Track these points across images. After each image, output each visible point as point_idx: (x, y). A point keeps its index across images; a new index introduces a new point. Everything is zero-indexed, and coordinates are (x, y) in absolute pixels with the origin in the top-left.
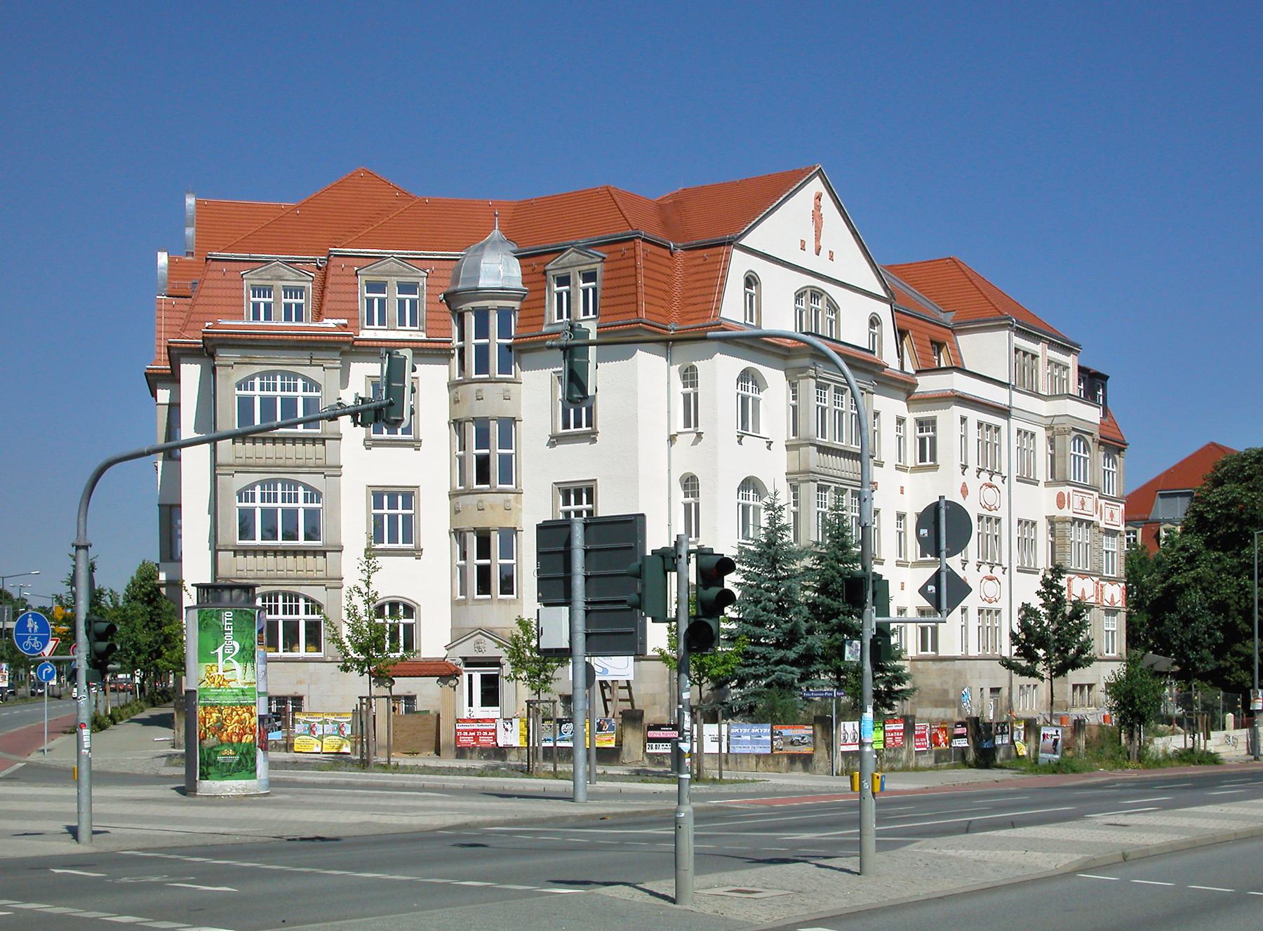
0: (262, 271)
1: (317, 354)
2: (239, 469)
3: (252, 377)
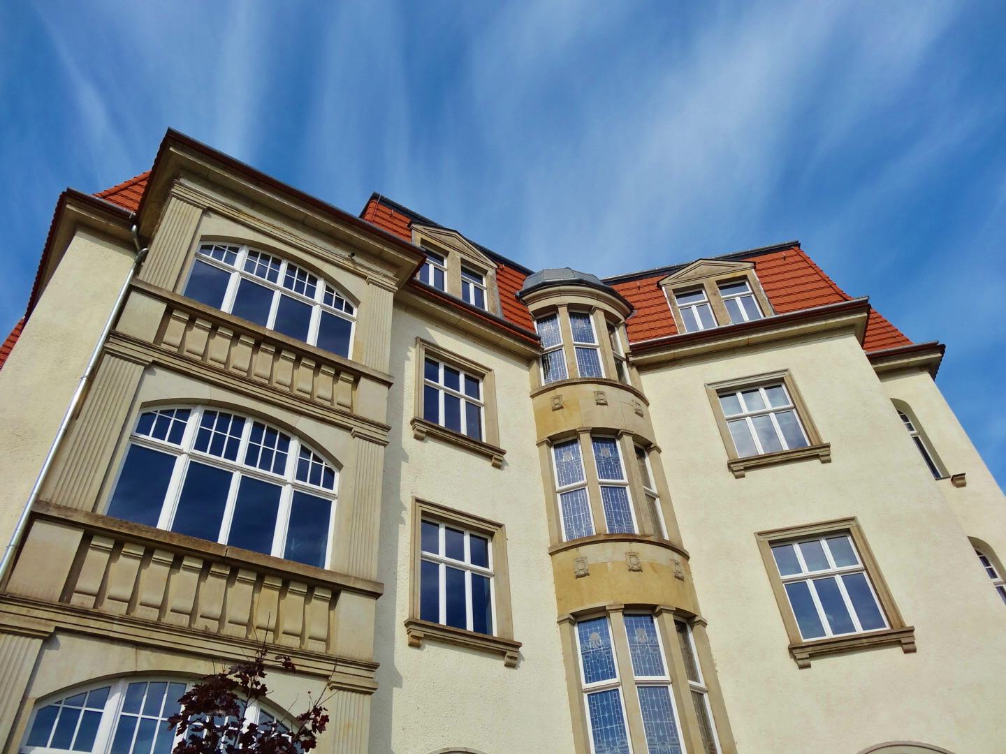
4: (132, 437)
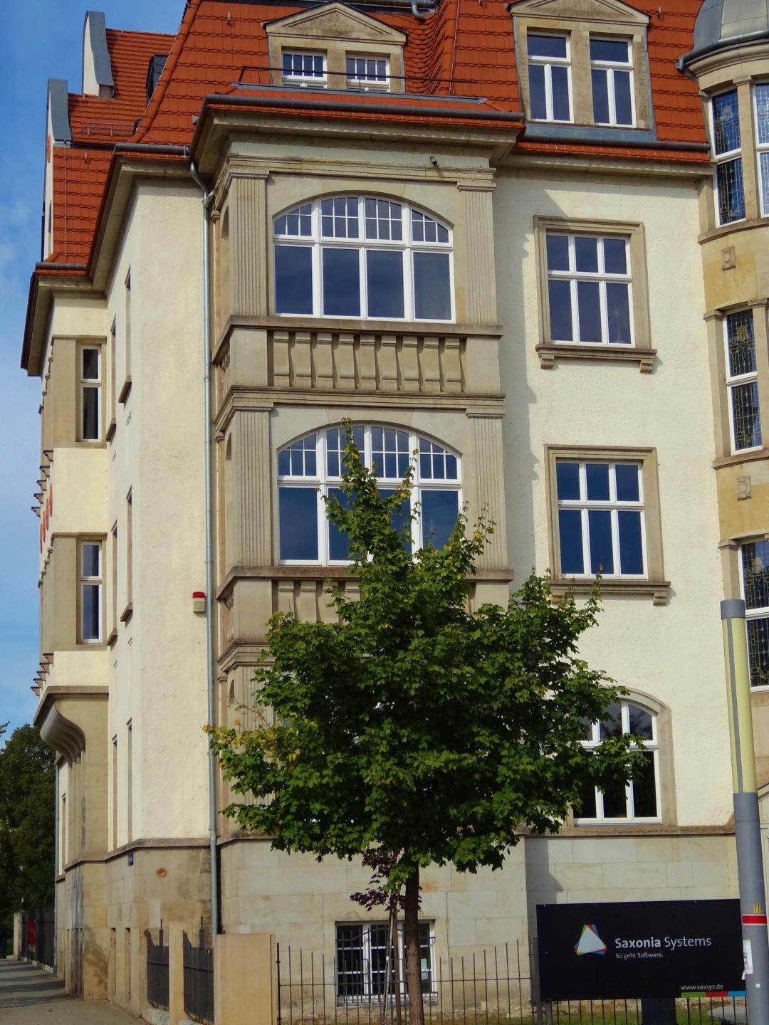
0: (305, 20)
1: (445, 160)
2: (285, 398)
3: (305, 205)
4: (279, 482)
